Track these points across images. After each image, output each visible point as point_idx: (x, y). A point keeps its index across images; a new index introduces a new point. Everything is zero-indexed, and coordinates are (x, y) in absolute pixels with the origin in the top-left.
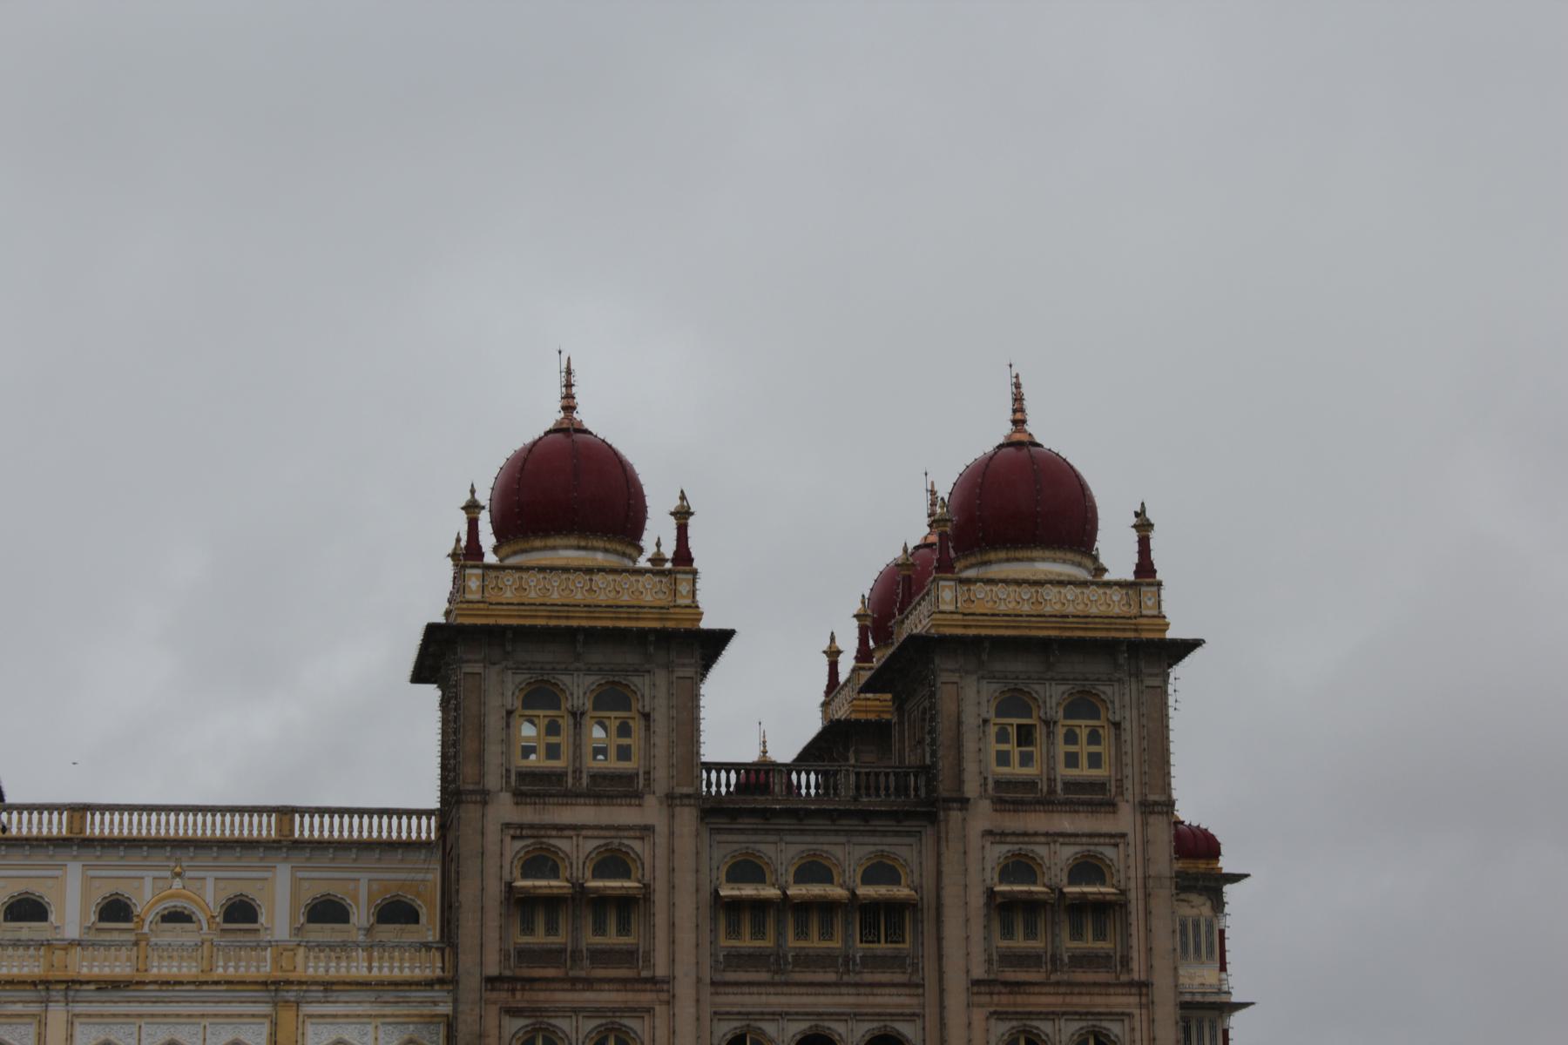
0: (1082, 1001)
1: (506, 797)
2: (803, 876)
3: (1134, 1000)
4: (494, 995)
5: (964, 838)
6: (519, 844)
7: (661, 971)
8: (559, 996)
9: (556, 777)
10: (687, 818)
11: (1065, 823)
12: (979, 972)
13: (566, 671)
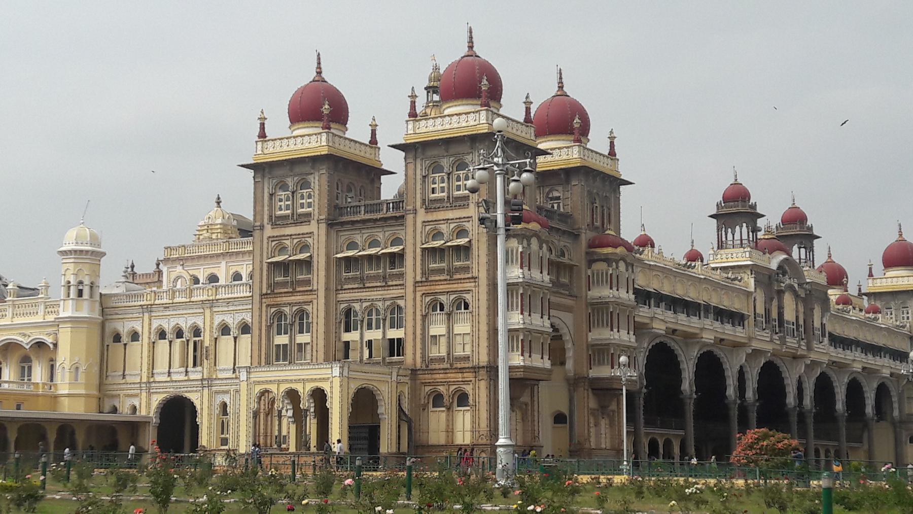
0: (455, 287)
1: (269, 226)
2: (371, 246)
3: (473, 284)
4: (264, 300)
5: (415, 224)
6: (274, 243)
7: (315, 288)
8: (284, 299)
9: (285, 217)
10: (323, 226)
11: (450, 215)
12: (418, 279)
13: (288, 176)
